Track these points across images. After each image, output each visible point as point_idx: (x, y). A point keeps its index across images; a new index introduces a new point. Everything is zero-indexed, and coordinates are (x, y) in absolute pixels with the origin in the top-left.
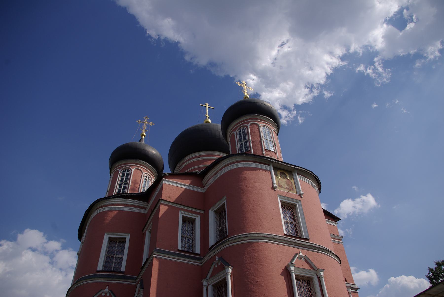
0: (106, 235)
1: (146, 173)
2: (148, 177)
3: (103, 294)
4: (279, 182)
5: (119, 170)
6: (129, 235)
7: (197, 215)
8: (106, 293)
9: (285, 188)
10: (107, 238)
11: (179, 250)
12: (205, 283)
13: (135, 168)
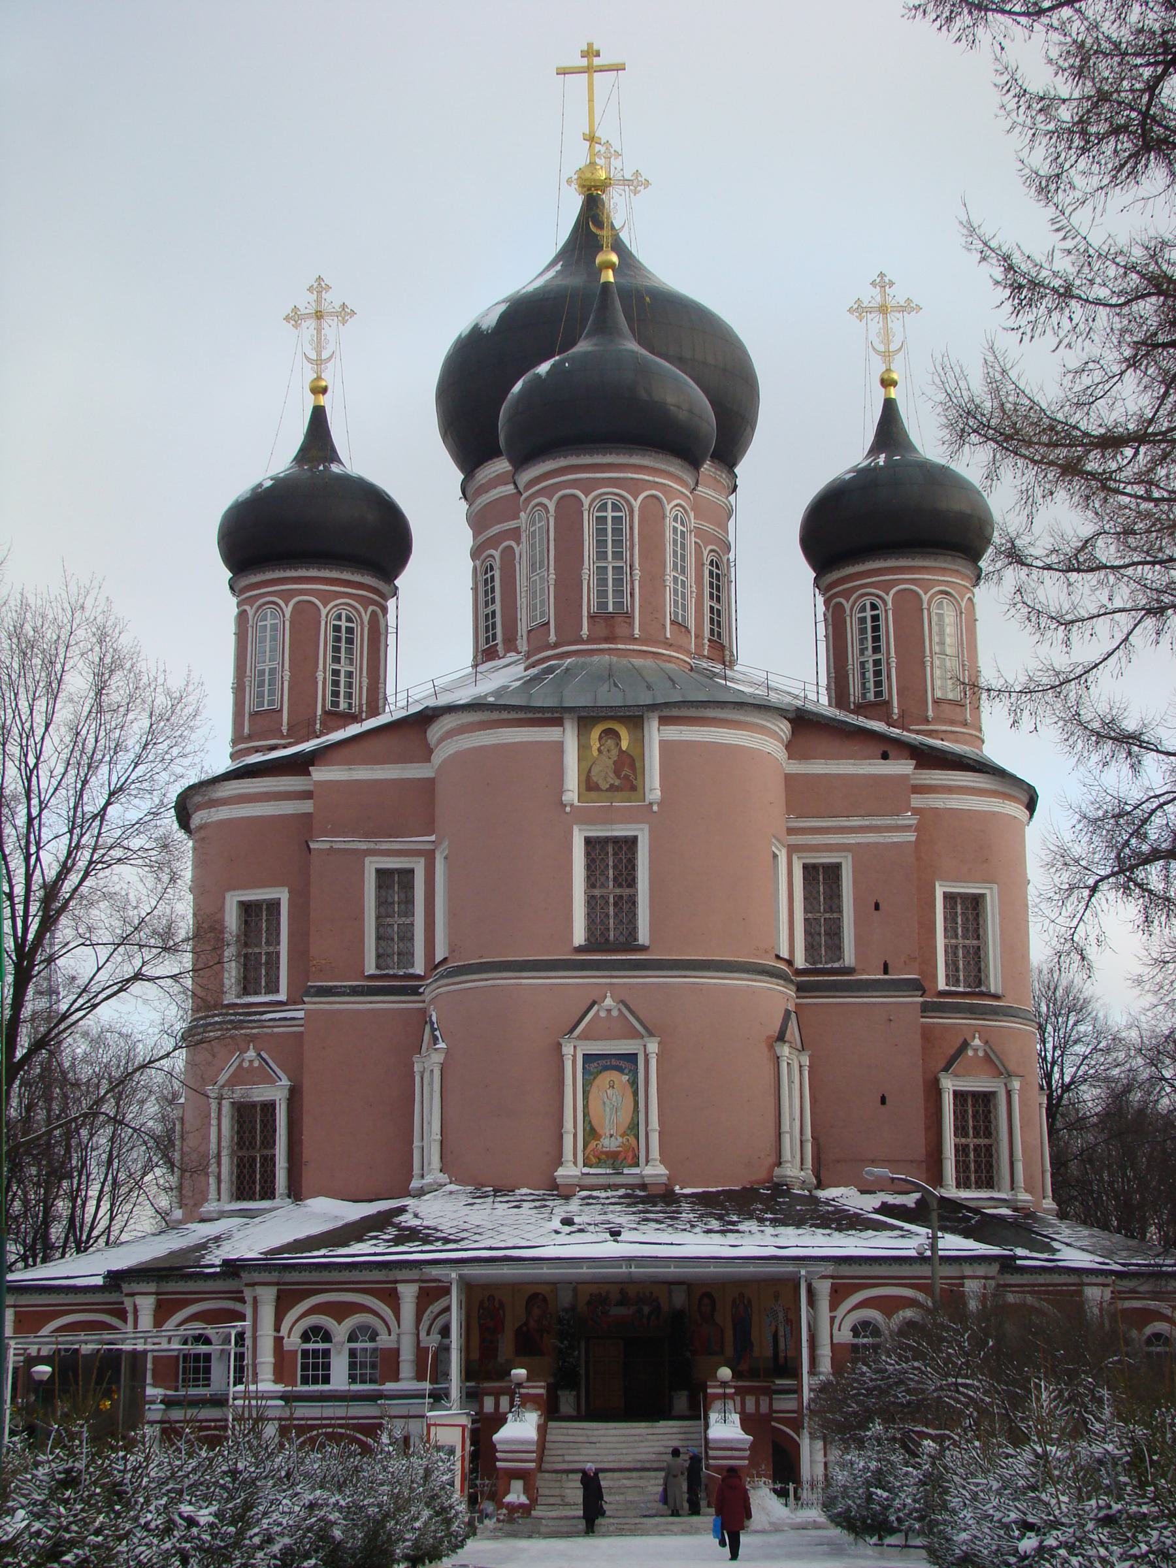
0: (228, 896)
1: (336, 606)
2: (344, 613)
3: (246, 1064)
4: (590, 771)
5: (247, 608)
6: (286, 890)
7: (415, 859)
8: (251, 1062)
9: (607, 790)
10: (235, 904)
11: (372, 977)
12: (417, 1068)
13: (291, 604)
